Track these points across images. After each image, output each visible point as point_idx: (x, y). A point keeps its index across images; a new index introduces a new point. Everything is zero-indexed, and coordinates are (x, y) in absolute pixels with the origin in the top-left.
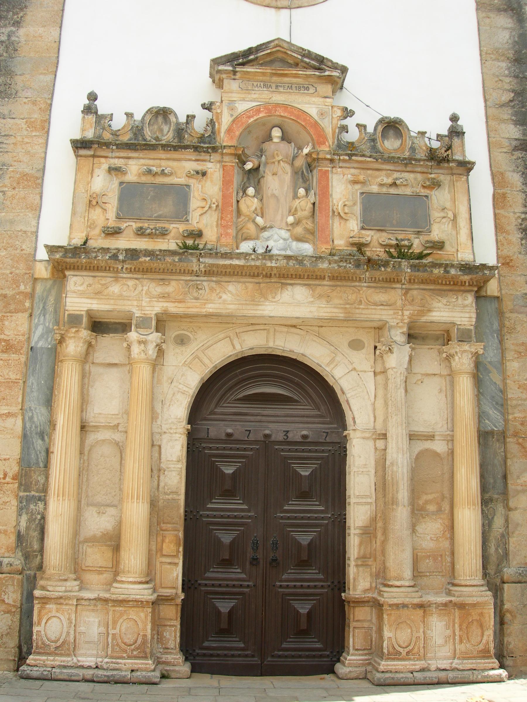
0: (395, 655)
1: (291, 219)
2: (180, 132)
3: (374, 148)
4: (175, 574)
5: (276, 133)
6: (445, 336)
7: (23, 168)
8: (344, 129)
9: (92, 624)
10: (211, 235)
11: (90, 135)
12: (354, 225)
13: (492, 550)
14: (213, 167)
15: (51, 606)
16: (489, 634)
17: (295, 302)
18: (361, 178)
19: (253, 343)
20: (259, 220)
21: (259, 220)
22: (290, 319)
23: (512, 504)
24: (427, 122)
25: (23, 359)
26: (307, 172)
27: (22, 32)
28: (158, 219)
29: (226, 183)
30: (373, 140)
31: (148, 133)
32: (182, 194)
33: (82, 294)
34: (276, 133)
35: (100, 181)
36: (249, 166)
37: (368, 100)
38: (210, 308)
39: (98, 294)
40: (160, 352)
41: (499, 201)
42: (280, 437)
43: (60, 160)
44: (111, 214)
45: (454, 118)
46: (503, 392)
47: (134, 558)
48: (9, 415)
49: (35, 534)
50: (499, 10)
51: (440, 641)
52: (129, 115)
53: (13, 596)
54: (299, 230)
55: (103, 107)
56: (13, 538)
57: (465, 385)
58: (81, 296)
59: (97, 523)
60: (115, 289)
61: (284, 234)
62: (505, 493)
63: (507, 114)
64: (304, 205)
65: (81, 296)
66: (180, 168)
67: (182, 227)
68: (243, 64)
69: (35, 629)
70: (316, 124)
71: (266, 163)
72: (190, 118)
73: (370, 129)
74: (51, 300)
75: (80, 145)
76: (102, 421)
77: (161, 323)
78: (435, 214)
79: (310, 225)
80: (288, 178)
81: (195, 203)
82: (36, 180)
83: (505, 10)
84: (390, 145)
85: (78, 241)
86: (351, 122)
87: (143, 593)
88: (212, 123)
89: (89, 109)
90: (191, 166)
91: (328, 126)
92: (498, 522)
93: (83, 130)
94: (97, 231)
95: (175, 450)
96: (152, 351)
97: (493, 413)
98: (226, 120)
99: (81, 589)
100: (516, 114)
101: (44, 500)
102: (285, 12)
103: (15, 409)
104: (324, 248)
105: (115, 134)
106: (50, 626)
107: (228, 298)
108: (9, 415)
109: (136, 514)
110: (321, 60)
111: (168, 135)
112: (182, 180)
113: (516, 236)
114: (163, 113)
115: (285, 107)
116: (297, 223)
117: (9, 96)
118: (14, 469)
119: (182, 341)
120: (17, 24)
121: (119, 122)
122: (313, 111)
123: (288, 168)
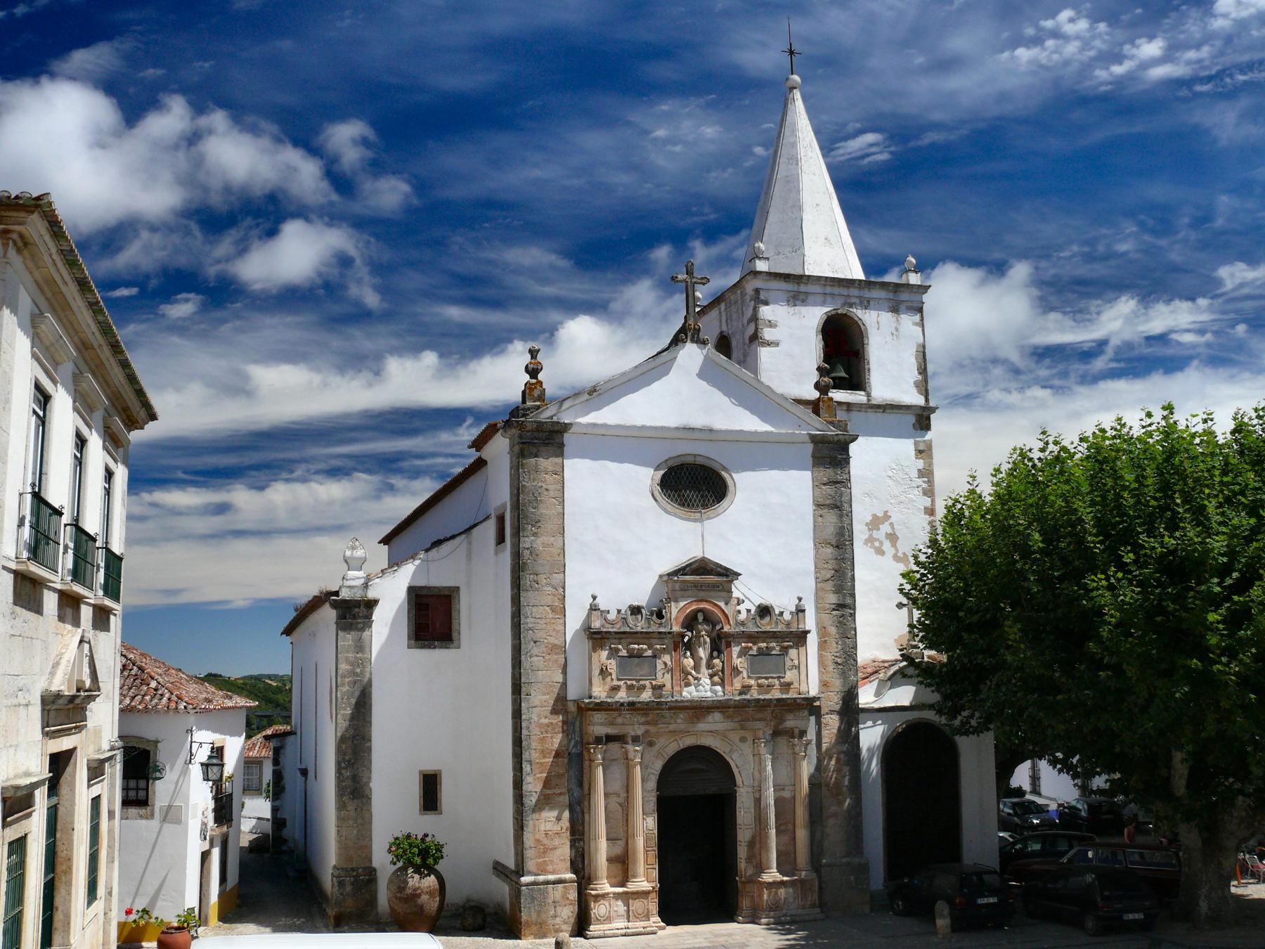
7: (552, 640)
8: (739, 612)
11: (597, 624)
16: (816, 896)
19: (689, 741)
22: (710, 733)
24: (783, 603)
25: (566, 761)
27: (539, 541)
33: (602, 724)
34: (700, 617)
37: (749, 593)
38: (672, 727)
39: (611, 724)
41: (822, 645)
44: (614, 676)
45: (800, 599)
48: (560, 794)
49: (579, 859)
52: (619, 611)
53: (573, 895)
54: (716, 679)
55: (602, 604)
60: (620, 720)
61: (708, 681)
63: (829, 586)
65: (598, 726)
74: (578, 723)
78: (788, 663)
80: (708, 646)
81: (660, 665)
86: (742, 608)
89: (594, 608)
92: (818, 834)
100: (835, 586)
101: (582, 840)
105: (612, 624)
106: (598, 909)
107: (680, 722)
108: (560, 794)
110: (727, 569)
113: (831, 667)
114: (636, 610)
117: (537, 590)
121: (612, 616)
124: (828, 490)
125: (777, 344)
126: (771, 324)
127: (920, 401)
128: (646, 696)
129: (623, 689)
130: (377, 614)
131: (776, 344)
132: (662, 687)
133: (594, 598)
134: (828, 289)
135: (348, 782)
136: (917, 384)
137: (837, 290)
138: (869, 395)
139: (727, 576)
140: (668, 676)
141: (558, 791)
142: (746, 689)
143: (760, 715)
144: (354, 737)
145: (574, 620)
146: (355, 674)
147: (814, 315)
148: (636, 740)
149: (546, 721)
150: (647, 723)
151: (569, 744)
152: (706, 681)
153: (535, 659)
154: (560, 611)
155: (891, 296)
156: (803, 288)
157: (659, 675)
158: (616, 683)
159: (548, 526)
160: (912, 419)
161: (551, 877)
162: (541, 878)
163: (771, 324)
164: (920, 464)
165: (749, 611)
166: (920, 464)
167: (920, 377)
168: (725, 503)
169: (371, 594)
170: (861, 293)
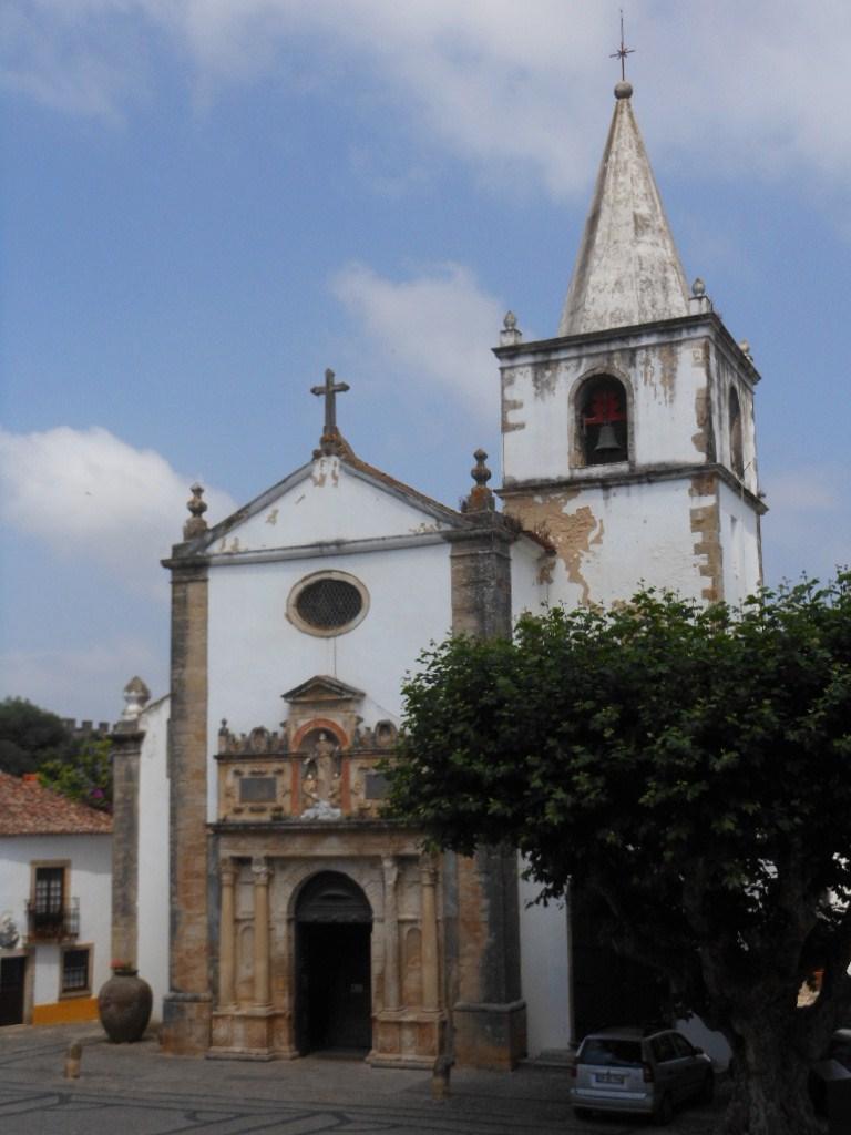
0: (383, 1050)
1: (330, 793)
2: (270, 743)
3: (375, 743)
4: (284, 1003)
5: (322, 737)
6: (413, 859)
8: (358, 731)
9: (239, 1029)
10: (288, 809)
11: (223, 749)
12: (362, 796)
13: (451, 990)
14: (286, 766)
15: (220, 1020)
16: (435, 1042)
17: (331, 847)
18: (365, 766)
19: (318, 867)
20: (314, 795)
21: (314, 795)
23: (461, 962)
26: (339, 760)
28: (263, 800)
29: (295, 775)
30: (374, 737)
31: (253, 746)
32: (271, 784)
33: (227, 848)
34: (322, 737)
35: (231, 780)
36: (308, 760)
40: (270, 877)
42: (341, 920)
43: (212, 767)
44: (237, 799)
46: (457, 891)
47: (260, 993)
48: (200, 915)
50: (469, 612)
51: (409, 1044)
54: (334, 801)
56: (206, 984)
57: (428, 892)
58: (227, 851)
59: (244, 973)
60: (242, 843)
62: (457, 956)
64: (336, 783)
66: (270, 768)
67: (274, 805)
68: (299, 696)
69: (214, 1032)
70: (341, 732)
71: (317, 758)
72: (275, 734)
73: (373, 730)
75: (219, 758)
76: (246, 916)
77: (269, 860)
79: (338, 797)
80: (328, 767)
81: (279, 790)
82: (202, 774)
83: (473, 612)
84: (385, 739)
85: (221, 817)
86: (362, 727)
87: (261, 1011)
88: (286, 736)
89: (224, 733)
90: (276, 766)
91: (348, 732)
92: (454, 974)
93: (220, 746)
94: (231, 810)
95: (282, 931)
96: (263, 879)
97: (452, 906)
98: (293, 733)
99: (238, 1009)
102: (332, 640)
103: (203, 911)
104: (347, 812)
106: (221, 1031)
107: (297, 847)
109: (261, 967)
110: (341, 689)
111: (263, 747)
112: (270, 775)
114: (259, 732)
115: (325, 721)
116: (333, 796)
118: (204, 944)
119: (283, 868)
120: (183, 666)
122: (339, 723)
123: (328, 760)
124: (469, 592)
125: (521, 426)
126: (516, 405)
127: (699, 458)
128: (266, 817)
129: (247, 811)
130: (146, 747)
131: (521, 426)
132: (280, 809)
133: (224, 722)
134: (586, 350)
135: (120, 901)
136: (695, 440)
137: (594, 350)
138: (632, 464)
139: (340, 694)
140: (288, 798)
141: (198, 912)
142: (363, 811)
143: (376, 840)
144: (125, 859)
145: (214, 746)
146: (128, 802)
147: (567, 378)
148: (258, 863)
149: (190, 843)
150: (266, 847)
151: (208, 865)
152: (325, 804)
153: (181, 784)
154: (203, 738)
155: (665, 339)
156: (554, 357)
157: (279, 797)
158: (238, 806)
159: (191, 658)
160: (688, 484)
161: (189, 996)
162: (181, 995)
163: (516, 405)
164: (698, 537)
165: (368, 729)
166: (698, 537)
167: (701, 431)
168: (359, 617)
169: (142, 727)
170: (625, 346)
